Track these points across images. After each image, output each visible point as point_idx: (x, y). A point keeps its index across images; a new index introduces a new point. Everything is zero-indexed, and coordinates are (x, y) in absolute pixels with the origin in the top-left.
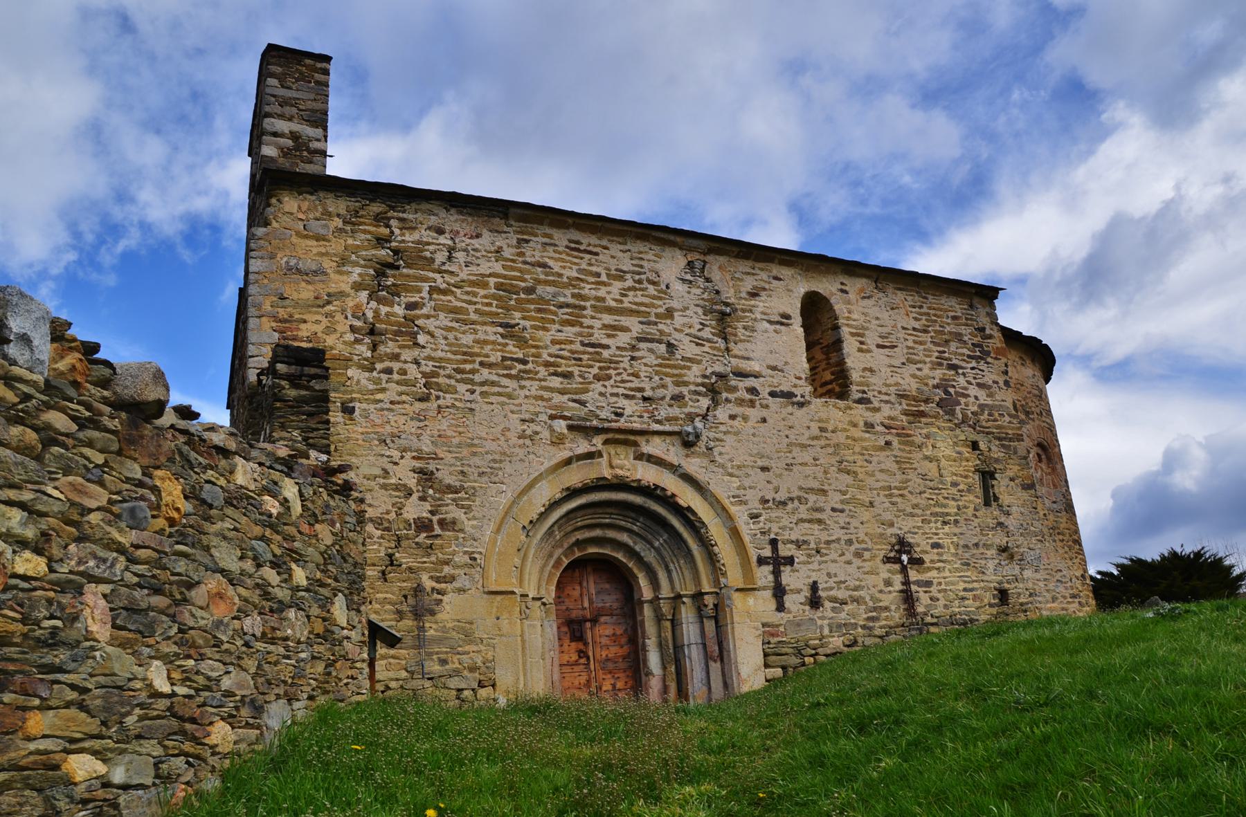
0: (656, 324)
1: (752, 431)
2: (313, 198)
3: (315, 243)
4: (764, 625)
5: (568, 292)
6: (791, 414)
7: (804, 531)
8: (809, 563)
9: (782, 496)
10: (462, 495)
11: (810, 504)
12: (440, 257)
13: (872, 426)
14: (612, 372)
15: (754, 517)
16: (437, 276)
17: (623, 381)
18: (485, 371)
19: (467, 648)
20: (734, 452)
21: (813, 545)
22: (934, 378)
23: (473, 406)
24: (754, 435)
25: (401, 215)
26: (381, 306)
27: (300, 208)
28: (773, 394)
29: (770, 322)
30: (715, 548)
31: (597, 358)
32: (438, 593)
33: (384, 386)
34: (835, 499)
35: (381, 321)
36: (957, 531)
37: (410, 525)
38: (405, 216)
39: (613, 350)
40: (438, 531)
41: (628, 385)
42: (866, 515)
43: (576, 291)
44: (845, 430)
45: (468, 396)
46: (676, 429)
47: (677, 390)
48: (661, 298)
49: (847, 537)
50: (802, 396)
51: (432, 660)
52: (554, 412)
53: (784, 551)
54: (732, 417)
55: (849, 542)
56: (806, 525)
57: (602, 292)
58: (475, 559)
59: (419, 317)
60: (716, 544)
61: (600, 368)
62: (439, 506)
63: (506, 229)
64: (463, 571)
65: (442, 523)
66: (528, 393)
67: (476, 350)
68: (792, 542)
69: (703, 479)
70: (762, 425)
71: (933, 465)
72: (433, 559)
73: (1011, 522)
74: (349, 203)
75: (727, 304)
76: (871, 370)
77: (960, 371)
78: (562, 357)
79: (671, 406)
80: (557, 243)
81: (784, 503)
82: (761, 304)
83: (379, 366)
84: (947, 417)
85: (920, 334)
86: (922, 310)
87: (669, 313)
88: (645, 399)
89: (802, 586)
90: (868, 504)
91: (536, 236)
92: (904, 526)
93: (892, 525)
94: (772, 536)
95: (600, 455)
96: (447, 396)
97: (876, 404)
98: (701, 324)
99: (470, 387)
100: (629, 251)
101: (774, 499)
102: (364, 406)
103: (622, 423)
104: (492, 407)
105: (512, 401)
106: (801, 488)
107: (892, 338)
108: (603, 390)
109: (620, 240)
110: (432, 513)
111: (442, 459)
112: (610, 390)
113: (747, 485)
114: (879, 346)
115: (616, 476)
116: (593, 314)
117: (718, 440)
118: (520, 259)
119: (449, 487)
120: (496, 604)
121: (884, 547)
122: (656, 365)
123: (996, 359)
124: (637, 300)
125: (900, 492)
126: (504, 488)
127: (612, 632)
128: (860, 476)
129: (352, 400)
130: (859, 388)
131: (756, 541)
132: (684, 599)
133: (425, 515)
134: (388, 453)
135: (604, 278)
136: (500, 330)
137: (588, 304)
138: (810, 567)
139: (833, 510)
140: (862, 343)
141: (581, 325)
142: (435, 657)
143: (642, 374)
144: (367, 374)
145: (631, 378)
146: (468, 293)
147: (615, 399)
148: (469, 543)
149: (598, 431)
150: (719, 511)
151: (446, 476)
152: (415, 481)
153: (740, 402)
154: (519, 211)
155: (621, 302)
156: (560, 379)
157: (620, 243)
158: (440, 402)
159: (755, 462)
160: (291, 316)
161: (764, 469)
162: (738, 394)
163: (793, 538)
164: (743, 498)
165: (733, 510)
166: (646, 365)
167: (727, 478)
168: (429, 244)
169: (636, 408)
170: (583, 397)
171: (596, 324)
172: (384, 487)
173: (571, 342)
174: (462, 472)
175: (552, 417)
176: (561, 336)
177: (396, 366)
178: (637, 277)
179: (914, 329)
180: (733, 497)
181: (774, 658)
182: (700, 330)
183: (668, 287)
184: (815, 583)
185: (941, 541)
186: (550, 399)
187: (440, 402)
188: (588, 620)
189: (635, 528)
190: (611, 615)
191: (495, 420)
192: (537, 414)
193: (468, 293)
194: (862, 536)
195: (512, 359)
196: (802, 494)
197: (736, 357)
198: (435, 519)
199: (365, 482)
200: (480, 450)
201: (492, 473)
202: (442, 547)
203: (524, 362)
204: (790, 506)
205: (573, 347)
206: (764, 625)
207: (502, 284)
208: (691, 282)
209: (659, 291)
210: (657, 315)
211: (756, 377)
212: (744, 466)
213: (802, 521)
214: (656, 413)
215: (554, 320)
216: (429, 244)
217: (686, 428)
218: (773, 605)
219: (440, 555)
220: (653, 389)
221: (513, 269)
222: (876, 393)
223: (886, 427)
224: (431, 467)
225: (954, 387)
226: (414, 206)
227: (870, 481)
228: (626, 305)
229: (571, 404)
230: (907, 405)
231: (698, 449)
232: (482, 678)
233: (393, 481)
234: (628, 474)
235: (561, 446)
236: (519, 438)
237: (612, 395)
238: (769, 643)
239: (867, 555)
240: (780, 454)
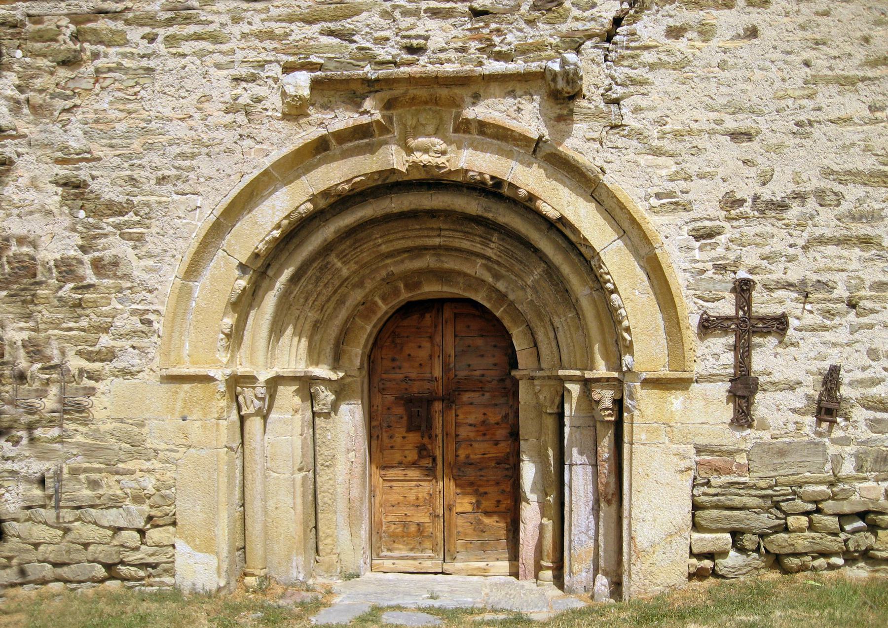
1: (721, 56)
4: (699, 451)
6: (826, 14)
7: (822, 263)
8: (825, 328)
9: (776, 190)
10: (131, 217)
11: (845, 206)
15: (704, 235)
19: (131, 465)
20: (671, 104)
23: (152, 64)
24: (722, 66)
30: (614, 296)
32: (89, 378)
37: (50, 270)
45: (144, 47)
46: (534, 66)
51: (79, 481)
52: (291, 59)
54: (675, 33)
56: (831, 250)
58: (149, 323)
60: (615, 291)
62: (95, 238)
64: (130, 342)
65: (98, 266)
66: (246, 28)
68: (789, 285)
69: (587, 163)
70: (745, 43)
72: (84, 323)
79: (531, 22)
81: (782, 206)
89: (801, 376)
94: (742, 274)
95: (384, 129)
96: (112, 50)
99: (147, 30)
103: (423, 66)
104: (183, 61)
105: (218, 47)
106: (827, 173)
110: (83, 249)
111: (99, 159)
115: (415, 166)
117: (634, 82)
119: (110, 205)
120: (182, 395)
126: (199, 201)
127: (481, 418)
131: (703, 285)
132: (568, 386)
133: (72, 253)
138: (828, 336)
142: (82, 477)
147: (410, 20)
148: (140, 296)
149: (371, 86)
150: (626, 225)
152: (58, 198)
158: (100, 63)
159: (719, 122)
161: (737, 136)
163: (793, 276)
164: (682, 198)
165: (653, 223)
167: (646, 160)
169: (454, 32)
170: (347, 24)
174: (132, 179)
175: (288, 69)
180: (658, 196)
181: (714, 513)
184: (834, 371)
186: (287, 35)
187: (100, 63)
188: (438, 399)
189: (489, 253)
190: (481, 390)
191: (188, 84)
192: (261, 65)
196: (824, 184)
200: (162, 139)
201: (178, 178)
202: (95, 304)
204: (795, 211)
206: (699, 451)
212: (690, 132)
213: (822, 241)
214: (497, 40)
217: (550, 64)
218: (728, 412)
219: (93, 316)
224: (83, 174)
231: (584, 103)
232: (154, 512)
234: (441, 160)
235: (302, 121)
236: (227, 112)
238: (708, 484)
240: (783, 103)
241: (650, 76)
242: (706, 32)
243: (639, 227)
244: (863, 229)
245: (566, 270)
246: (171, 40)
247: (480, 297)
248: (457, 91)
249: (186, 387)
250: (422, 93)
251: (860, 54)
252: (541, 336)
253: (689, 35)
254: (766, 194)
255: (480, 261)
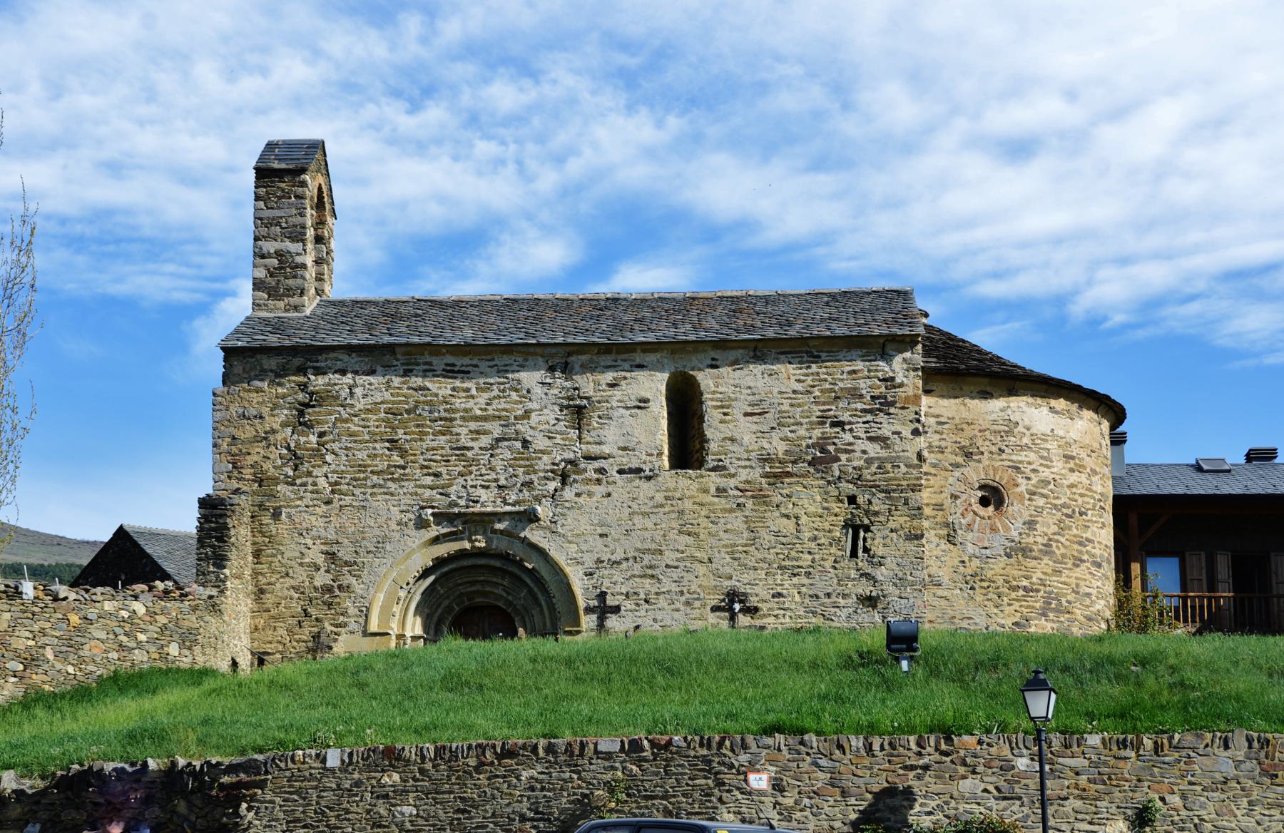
0: (514, 424)
2: (254, 360)
3: (256, 394)
5: (441, 408)
9: (618, 556)
11: (644, 563)
12: (344, 393)
13: (725, 490)
14: (474, 468)
16: (341, 409)
17: (481, 475)
18: (375, 478)
20: (576, 523)
21: (642, 596)
22: (810, 438)
25: (315, 364)
26: (301, 438)
27: (244, 369)
28: (620, 472)
29: (627, 408)
31: (461, 458)
32: (336, 634)
33: (302, 494)
34: (670, 557)
35: (300, 449)
36: (806, 581)
38: (318, 364)
39: (477, 450)
40: (337, 592)
41: (485, 478)
42: (701, 569)
43: (449, 406)
44: (692, 497)
47: (527, 478)
48: (521, 402)
49: (678, 589)
50: (651, 470)
52: (425, 504)
53: (610, 601)
54: (578, 495)
55: (682, 593)
56: (637, 580)
57: (470, 404)
59: (327, 442)
60: (554, 597)
61: (464, 466)
63: (395, 363)
65: (340, 587)
66: (405, 491)
67: (369, 462)
71: (790, 525)
73: (881, 573)
74: (278, 361)
75: (586, 398)
76: (732, 440)
77: (847, 427)
78: (434, 461)
80: (435, 368)
81: (619, 563)
82: (620, 393)
83: (298, 481)
84: (819, 475)
85: (800, 396)
86: (810, 371)
87: (527, 414)
88: (499, 487)
90: (706, 560)
91: (418, 364)
92: (740, 581)
93: (731, 578)
96: (346, 498)
97: (733, 471)
98: (557, 419)
99: (363, 490)
100: (496, 365)
101: (609, 560)
102: (289, 510)
103: (477, 509)
106: (637, 550)
107: (765, 405)
108: (464, 483)
109: (489, 357)
112: (470, 483)
113: (584, 549)
114: (746, 414)
116: (461, 423)
118: (406, 386)
121: (718, 597)
122: (510, 459)
123: (903, 408)
124: (499, 407)
125: (745, 549)
128: (702, 536)
129: (280, 507)
130: (714, 457)
133: (328, 582)
134: (303, 542)
135: (474, 392)
136: (387, 445)
137: (457, 415)
139: (667, 566)
140: (725, 414)
141: (451, 433)
143: (498, 468)
144: (290, 488)
145: (489, 472)
146: (363, 420)
147: (473, 490)
151: (345, 553)
153: (588, 481)
154: (403, 349)
155: (486, 410)
156: (432, 478)
157: (488, 360)
160: (240, 451)
161: (601, 535)
162: (587, 475)
164: (580, 560)
166: (502, 460)
168: (335, 384)
171: (463, 432)
172: (301, 564)
173: (442, 448)
176: (435, 444)
177: (310, 480)
178: (502, 387)
179: (794, 392)
180: (571, 559)
182: (554, 425)
183: (529, 391)
185: (785, 591)
189: (505, 583)
193: (363, 420)
194: (693, 588)
195: (395, 466)
196: (636, 554)
197: (588, 443)
198: (335, 585)
199: (289, 562)
203: (404, 468)
204: (625, 565)
205: (444, 452)
207: (390, 408)
208: (550, 384)
209: (520, 397)
210: (516, 418)
211: (605, 458)
213: (634, 576)
214: (507, 497)
215: (429, 432)
216: (335, 384)
220: (506, 479)
221: (398, 395)
222: (734, 460)
223: (741, 491)
224: (335, 549)
225: (834, 444)
226: (324, 356)
227: (713, 541)
228: (490, 412)
229: (438, 496)
230: (770, 467)
233: (307, 560)
237: (472, 486)
239: (697, 604)
241: (568, 513)
242: (590, 494)
243: (563, 571)
244: (650, 572)
245: (536, 589)
246: (372, 494)
247: (501, 604)
248: (492, 518)
249: (378, 637)
250: (478, 518)
251: (651, 503)
252: (527, 620)
253: (584, 496)
254: (613, 558)
255: (501, 587)
